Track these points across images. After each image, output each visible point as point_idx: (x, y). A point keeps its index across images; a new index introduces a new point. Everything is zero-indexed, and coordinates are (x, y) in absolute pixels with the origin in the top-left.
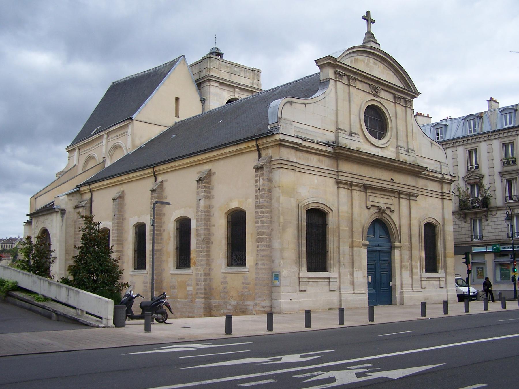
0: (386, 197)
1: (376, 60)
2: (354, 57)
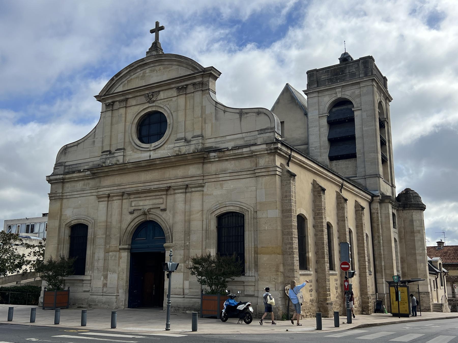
0: (154, 197)
1: (153, 66)
2: (128, 80)
